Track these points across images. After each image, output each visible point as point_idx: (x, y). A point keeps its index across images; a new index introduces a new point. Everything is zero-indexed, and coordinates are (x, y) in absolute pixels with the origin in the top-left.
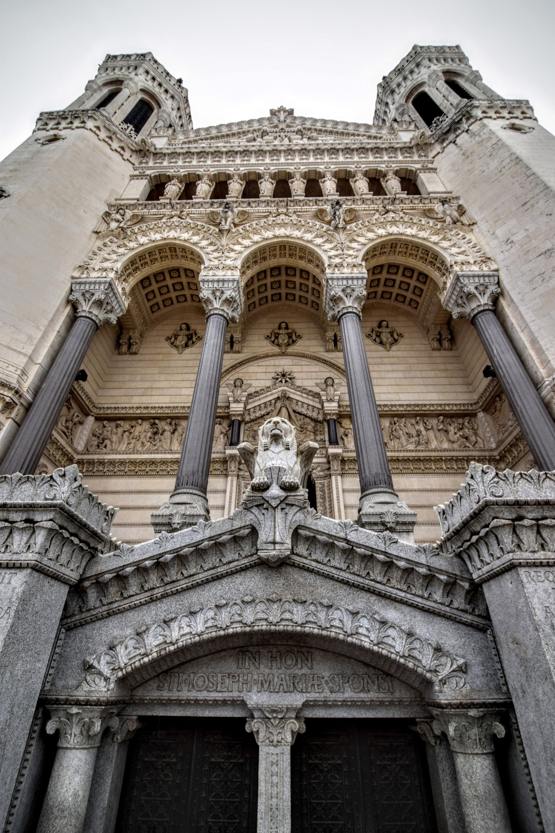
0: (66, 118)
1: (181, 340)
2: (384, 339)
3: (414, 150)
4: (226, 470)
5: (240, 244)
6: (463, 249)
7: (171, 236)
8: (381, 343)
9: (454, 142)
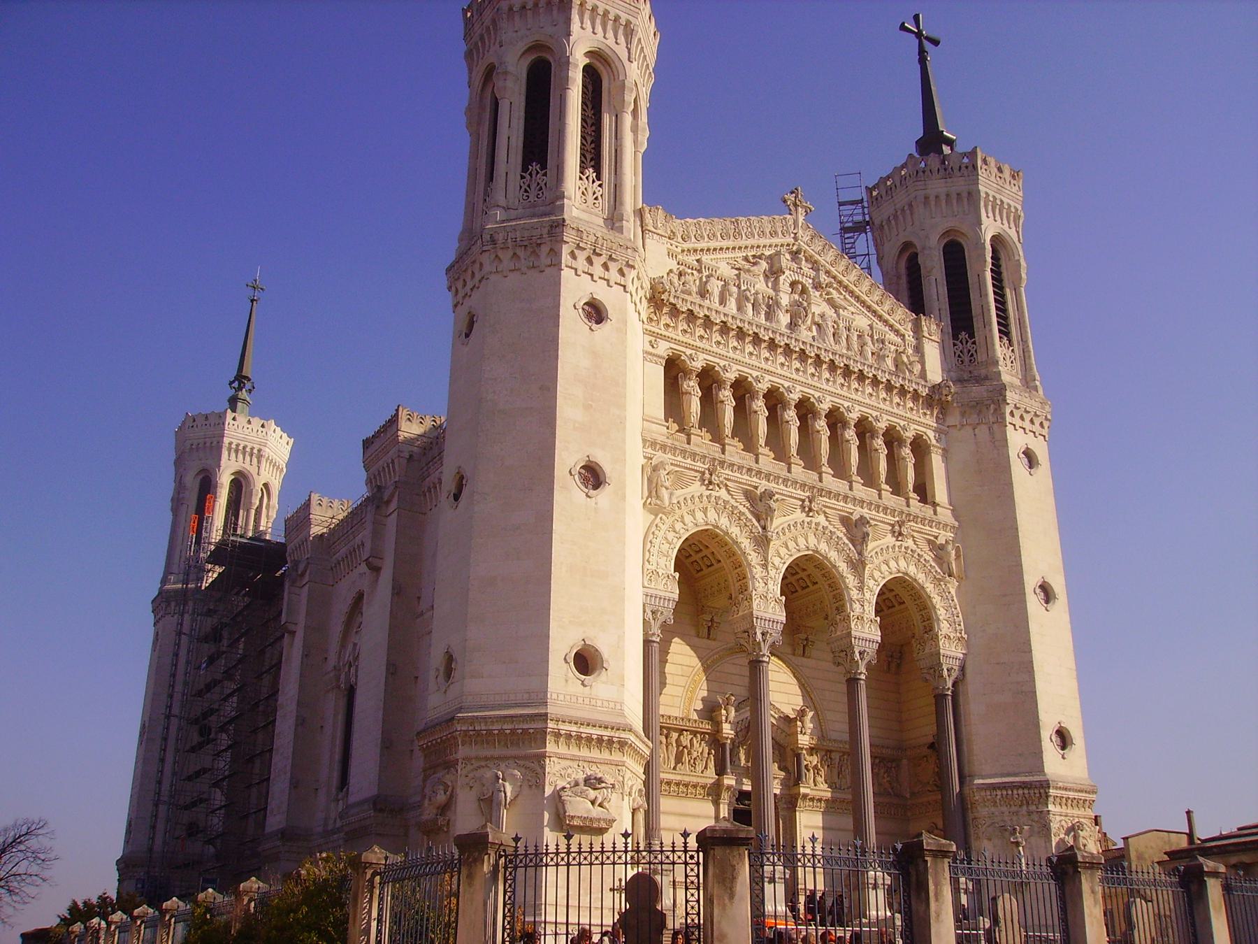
0: (601, 255)
9: (974, 429)
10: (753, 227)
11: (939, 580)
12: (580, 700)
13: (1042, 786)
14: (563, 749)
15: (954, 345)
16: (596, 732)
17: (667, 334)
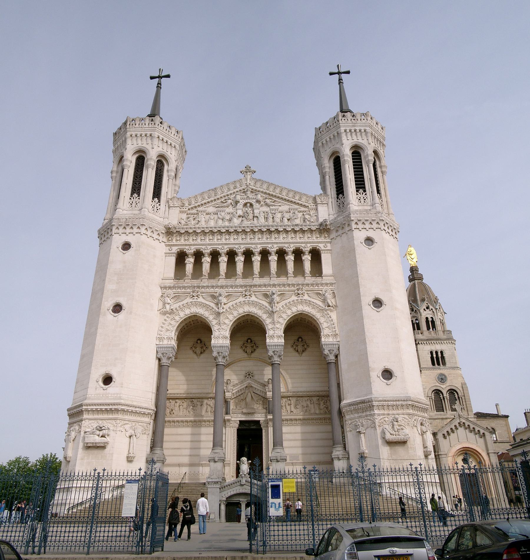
1: (198, 350)
2: (299, 351)
3: (322, 231)
4: (225, 424)
5: (228, 318)
6: (329, 325)
7: (195, 312)
8: (297, 351)
10: (224, 189)
11: (323, 310)
12: (101, 396)
13: (369, 402)
14: (91, 416)
15: (337, 201)
16: (104, 407)
17: (177, 243)
